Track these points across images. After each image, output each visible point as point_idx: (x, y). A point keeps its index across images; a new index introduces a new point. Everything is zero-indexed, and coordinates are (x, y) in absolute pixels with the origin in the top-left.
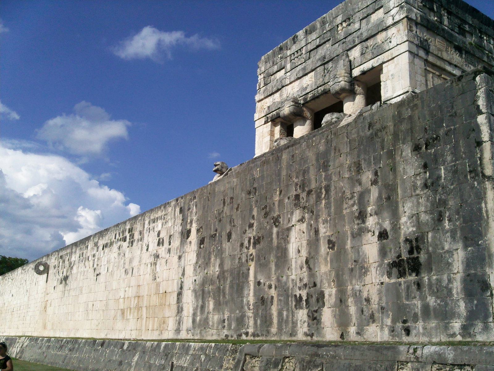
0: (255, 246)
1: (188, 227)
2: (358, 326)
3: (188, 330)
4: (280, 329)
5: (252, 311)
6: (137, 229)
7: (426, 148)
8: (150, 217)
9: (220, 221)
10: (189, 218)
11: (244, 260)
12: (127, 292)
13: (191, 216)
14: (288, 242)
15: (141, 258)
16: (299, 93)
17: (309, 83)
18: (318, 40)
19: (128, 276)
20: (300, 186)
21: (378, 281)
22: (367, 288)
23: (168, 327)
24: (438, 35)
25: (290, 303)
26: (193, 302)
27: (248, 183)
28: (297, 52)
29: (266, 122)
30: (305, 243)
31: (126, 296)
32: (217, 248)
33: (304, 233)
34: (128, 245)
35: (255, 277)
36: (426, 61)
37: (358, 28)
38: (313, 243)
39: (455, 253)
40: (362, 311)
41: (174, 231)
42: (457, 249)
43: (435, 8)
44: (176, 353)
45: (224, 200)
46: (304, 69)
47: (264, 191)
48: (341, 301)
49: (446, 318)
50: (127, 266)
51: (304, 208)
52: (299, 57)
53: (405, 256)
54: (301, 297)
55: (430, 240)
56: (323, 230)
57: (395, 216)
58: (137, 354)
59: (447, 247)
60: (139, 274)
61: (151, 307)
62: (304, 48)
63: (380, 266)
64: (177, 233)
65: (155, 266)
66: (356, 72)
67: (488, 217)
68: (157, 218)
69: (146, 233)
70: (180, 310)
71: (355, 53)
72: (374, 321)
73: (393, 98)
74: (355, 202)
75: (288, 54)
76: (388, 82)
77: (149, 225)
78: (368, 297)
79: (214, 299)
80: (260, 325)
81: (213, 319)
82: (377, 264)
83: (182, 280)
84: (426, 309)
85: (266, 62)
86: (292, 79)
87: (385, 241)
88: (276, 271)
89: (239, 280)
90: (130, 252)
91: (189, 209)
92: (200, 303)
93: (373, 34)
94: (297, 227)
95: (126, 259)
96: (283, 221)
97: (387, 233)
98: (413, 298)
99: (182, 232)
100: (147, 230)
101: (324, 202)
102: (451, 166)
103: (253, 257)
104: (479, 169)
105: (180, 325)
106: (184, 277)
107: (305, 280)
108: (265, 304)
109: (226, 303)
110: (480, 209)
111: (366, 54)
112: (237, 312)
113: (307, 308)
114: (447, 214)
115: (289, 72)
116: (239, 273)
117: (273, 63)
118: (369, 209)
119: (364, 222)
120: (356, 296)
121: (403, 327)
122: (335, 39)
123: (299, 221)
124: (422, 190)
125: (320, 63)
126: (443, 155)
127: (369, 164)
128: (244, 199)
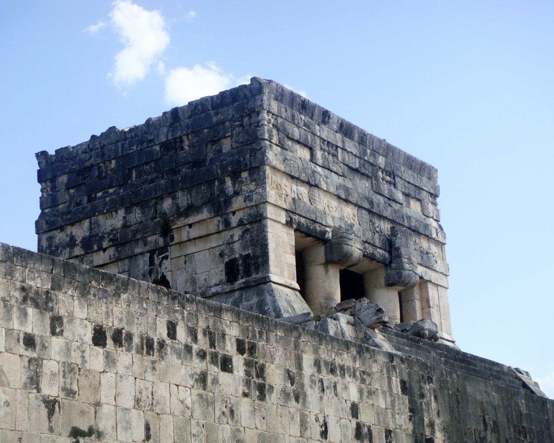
10: (426, 415)
27: (514, 414)
28: (328, 142)
34: (241, 388)
41: (395, 422)
77: (319, 371)
100: (313, 382)
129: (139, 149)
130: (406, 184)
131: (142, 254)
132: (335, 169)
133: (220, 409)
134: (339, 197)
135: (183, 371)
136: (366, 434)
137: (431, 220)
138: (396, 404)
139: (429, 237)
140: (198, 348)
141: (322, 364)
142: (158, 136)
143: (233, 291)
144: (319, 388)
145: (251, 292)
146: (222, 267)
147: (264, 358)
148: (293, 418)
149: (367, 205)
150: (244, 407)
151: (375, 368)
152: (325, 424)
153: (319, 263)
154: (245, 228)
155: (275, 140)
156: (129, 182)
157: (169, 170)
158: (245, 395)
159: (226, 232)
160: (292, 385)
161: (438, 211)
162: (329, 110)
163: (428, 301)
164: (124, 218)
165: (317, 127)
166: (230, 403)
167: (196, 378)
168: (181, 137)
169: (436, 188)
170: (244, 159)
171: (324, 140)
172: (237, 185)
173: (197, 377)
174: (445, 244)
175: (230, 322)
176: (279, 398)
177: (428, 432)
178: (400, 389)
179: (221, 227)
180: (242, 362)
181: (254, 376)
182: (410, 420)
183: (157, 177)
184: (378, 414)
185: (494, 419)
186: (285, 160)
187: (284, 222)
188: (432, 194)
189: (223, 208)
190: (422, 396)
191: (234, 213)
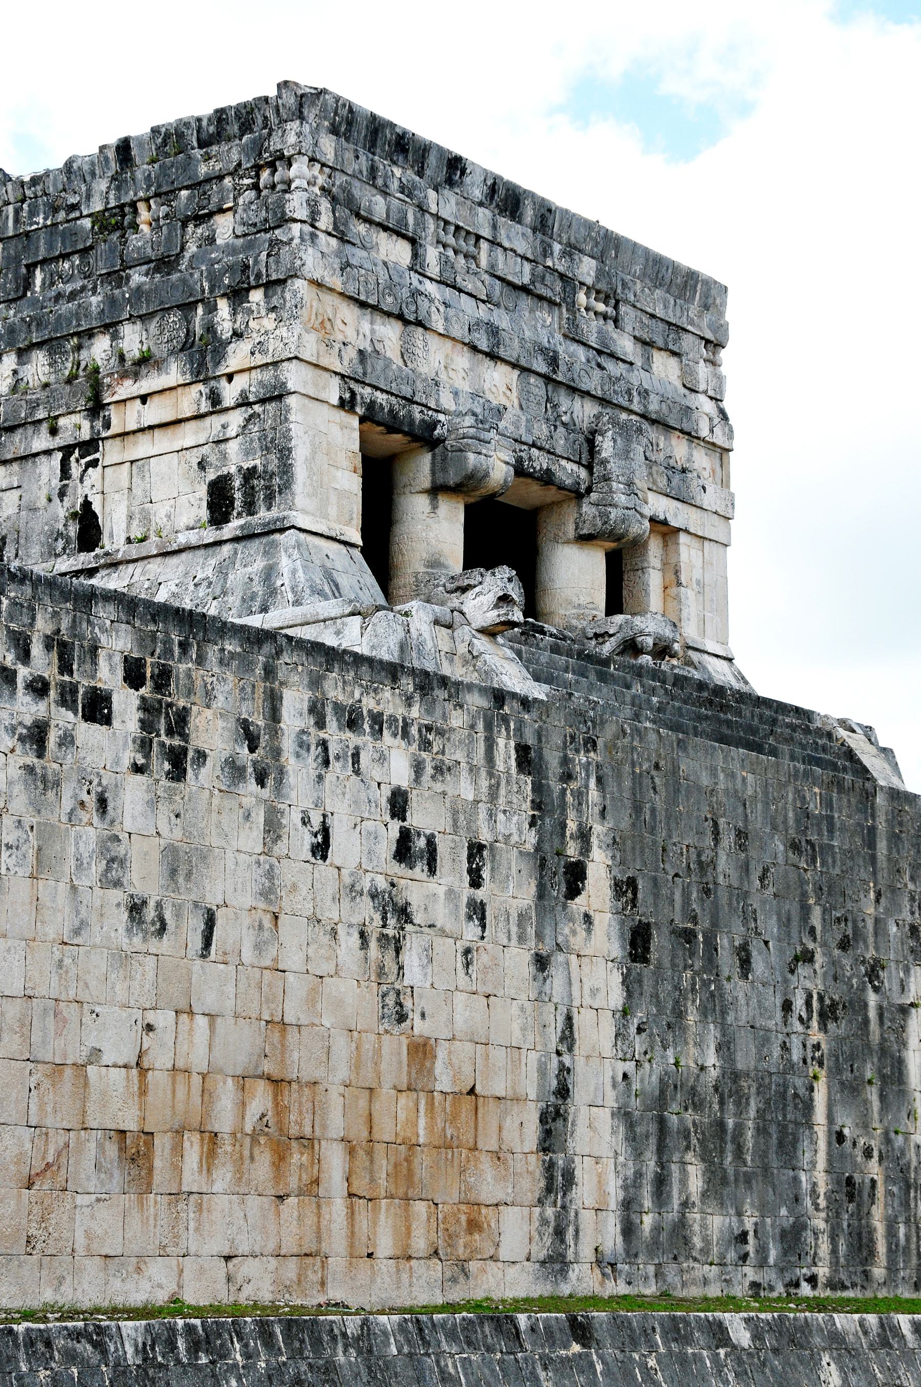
0: (825, 1025)
1: (572, 850)
4: (892, 1268)
5: (823, 1215)
10: (571, 814)
11: (796, 1055)
13: (579, 811)
15: (270, 874)
19: (165, 945)
26: (621, 1159)
27: (791, 814)
28: (458, 228)
31: (160, 1059)
32: (706, 984)
34: (130, 755)
41: (493, 829)
45: (716, 824)
47: (837, 871)
60: (268, 963)
61: (380, 1149)
65: (391, 953)
70: (558, 1182)
77: (321, 724)
79: (703, 1160)
80: (846, 1256)
81: (704, 1226)
83: (567, 1059)
89: (785, 1116)
91: (567, 777)
92: (651, 1166)
96: (890, 978)
100: (303, 745)
105: (563, 1241)
106: (570, 1049)
108: (857, 1198)
109: (748, 1180)
112: (784, 1212)
116: (785, 1092)
128: (781, 860)
129: (49, 222)
130: (645, 319)
131: (48, 452)
132: (470, 287)
133: (75, 796)
134: (474, 349)
136: (422, 851)
137: (702, 398)
138: (502, 791)
139: (691, 436)
140: (31, 674)
141: (329, 710)
142: (89, 197)
143: (219, 543)
144: (317, 757)
145: (255, 545)
146: (202, 491)
147: (188, 696)
148: (247, 817)
149: (541, 366)
150: (132, 795)
151: (457, 719)
152: (325, 831)
153: (418, 489)
154: (250, 411)
155: (325, 221)
156: (29, 294)
157: (109, 274)
158: (138, 769)
159: (214, 418)
160: (252, 750)
161: (720, 379)
162: (464, 155)
163: (677, 572)
164: (15, 372)
165: (432, 194)
166: (100, 784)
167: (21, 734)
168: (133, 205)
169: (721, 328)
170: (256, 262)
171: (447, 223)
172: (239, 317)
173: (25, 731)
174: (729, 450)
175: (112, 622)
176: (218, 777)
177: (572, 850)
178: (513, 763)
179: (205, 407)
181: (162, 732)
182: (532, 824)
183: (83, 288)
184: (455, 813)
185: (741, 824)
186: (346, 266)
187: (335, 401)
188: (708, 342)
189: (210, 365)
190: (567, 777)
191: (230, 377)
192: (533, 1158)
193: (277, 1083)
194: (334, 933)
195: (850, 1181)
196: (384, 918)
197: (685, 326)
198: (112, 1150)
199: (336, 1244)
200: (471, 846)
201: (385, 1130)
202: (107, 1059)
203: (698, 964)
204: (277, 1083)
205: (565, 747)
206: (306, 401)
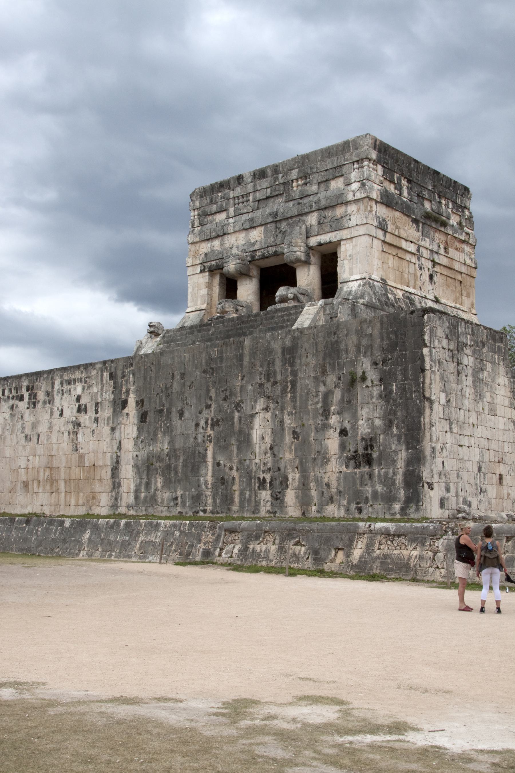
0: (213, 428)
1: (124, 397)
2: (318, 506)
3: (128, 507)
5: (210, 490)
6: (41, 388)
7: (382, 365)
8: (62, 377)
9: (168, 396)
10: (124, 387)
11: (200, 440)
12: (31, 461)
13: (126, 385)
14: (252, 428)
15: (51, 423)
16: (246, 247)
17: (259, 239)
18: (269, 190)
20: (265, 376)
21: (337, 470)
22: (328, 475)
23: (100, 502)
24: (397, 211)
25: (253, 484)
27: (204, 361)
28: (242, 196)
29: (201, 271)
30: (269, 431)
31: (30, 466)
32: (165, 424)
33: (268, 421)
34: (26, 406)
35: (214, 458)
36: (384, 241)
37: (316, 192)
38: (278, 432)
39: (399, 453)
40: (323, 494)
41: (101, 398)
42: (401, 450)
43: (396, 180)
44: (143, 530)
45: (173, 374)
46: (252, 220)
47: (224, 374)
48: (304, 485)
49: (390, 502)
50: (28, 431)
51: (269, 398)
52: (245, 204)
53: (361, 451)
54: (264, 480)
55: (381, 441)
56: (288, 421)
57: (355, 418)
58: (87, 532)
59: (393, 448)
60: (49, 443)
61: (72, 481)
62: (252, 195)
63: (340, 457)
64: (107, 402)
65: (75, 435)
66: (313, 241)
67: (425, 429)
68: (74, 380)
69: (57, 395)
70: (116, 485)
71: (312, 219)
72: (332, 502)
73: (349, 281)
74: (319, 400)
75: (232, 196)
76: (346, 262)
77: (62, 386)
78: (328, 482)
79: (163, 477)
80: (220, 503)
81: (162, 496)
82: (337, 456)
83: (119, 454)
84: (375, 494)
85: (201, 197)
86: (237, 228)
87: (345, 437)
88: (238, 454)
89: (194, 460)
90: (32, 415)
91: (123, 377)
92: (145, 480)
93: (332, 205)
94: (261, 414)
95: (25, 423)
96: (246, 406)
97: (346, 431)
98: (365, 485)
99: (115, 402)
100: (58, 392)
101: (289, 395)
102: (401, 384)
103: (212, 438)
104: (421, 390)
106: (120, 451)
107: (269, 465)
108: (226, 484)
109: (179, 481)
110: (420, 422)
111: (324, 225)
112: (193, 490)
113: (270, 490)
114: (396, 422)
115: (232, 217)
116: (195, 452)
117: (211, 200)
118: (332, 408)
119: (327, 419)
120: (318, 481)
121: (357, 507)
122: (289, 196)
123: (263, 409)
124: (377, 399)
125: (270, 219)
126: (395, 374)
127: (333, 369)
128: (198, 377)
134: (245, 229)
135: (6, 406)
148: (47, 412)
150: (27, 413)
152: (62, 410)
158: (28, 408)
162: (241, 173)
180: (28, 394)
182: (113, 392)
184: (92, 397)
192: (109, 481)
193: (51, 468)
194: (63, 433)
195: (222, 478)
196: (74, 427)
197: (343, 163)
198: (22, 485)
199: (62, 502)
200: (96, 404)
201: (73, 477)
202: (22, 467)
203: (163, 419)
204: (51, 468)
205: (123, 368)
206: (192, 276)
